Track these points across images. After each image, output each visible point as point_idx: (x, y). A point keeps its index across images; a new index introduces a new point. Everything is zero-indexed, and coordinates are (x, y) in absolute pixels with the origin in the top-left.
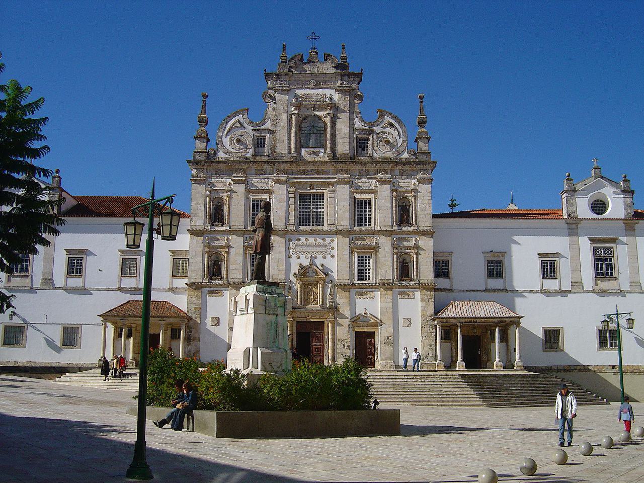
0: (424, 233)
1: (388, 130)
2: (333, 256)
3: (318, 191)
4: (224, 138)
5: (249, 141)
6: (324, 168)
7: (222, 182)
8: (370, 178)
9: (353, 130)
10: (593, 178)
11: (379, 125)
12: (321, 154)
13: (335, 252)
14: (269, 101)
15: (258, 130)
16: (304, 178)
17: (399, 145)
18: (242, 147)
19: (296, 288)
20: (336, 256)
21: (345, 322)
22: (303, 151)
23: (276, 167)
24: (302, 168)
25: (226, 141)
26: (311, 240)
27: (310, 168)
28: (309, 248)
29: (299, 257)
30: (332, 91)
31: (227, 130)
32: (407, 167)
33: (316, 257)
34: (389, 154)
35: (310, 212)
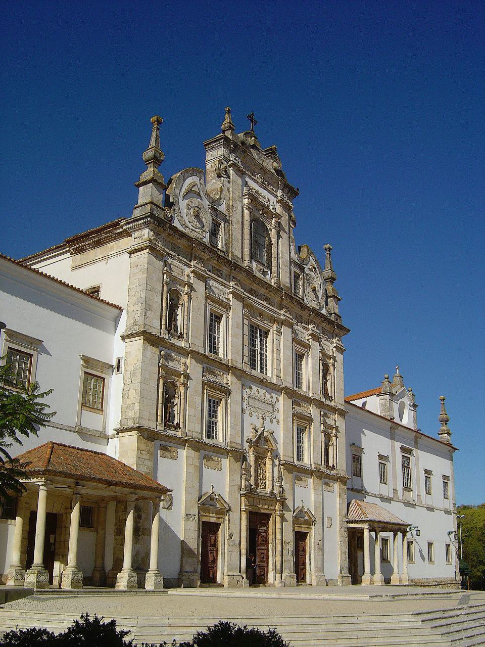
0: (342, 413)
1: (312, 273)
4: (181, 199)
5: (206, 218)
6: (271, 296)
8: (304, 328)
9: (291, 261)
10: (399, 386)
11: (306, 265)
12: (268, 277)
13: (281, 416)
14: (224, 176)
15: (216, 210)
17: (320, 297)
18: (198, 225)
19: (248, 459)
21: (289, 516)
23: (234, 273)
24: (255, 287)
25: (183, 204)
26: (262, 391)
27: (262, 290)
30: (275, 200)
31: (184, 190)
32: (328, 327)
34: (314, 305)
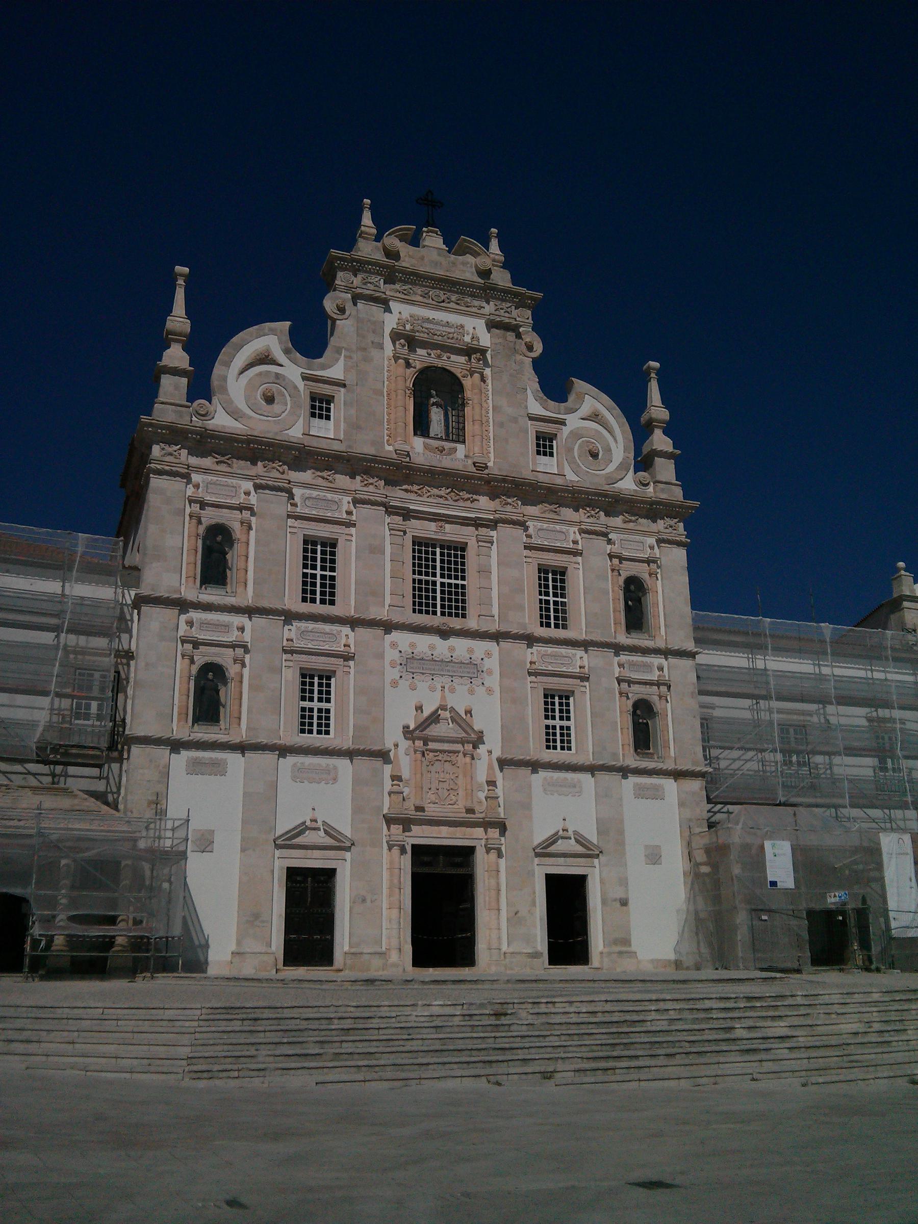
2: (490, 691)
3: (451, 533)
7: (227, 486)
13: (493, 681)
16: (423, 503)
20: (497, 689)
22: (418, 443)
28: (437, 667)
29: (413, 688)
33: (452, 690)
35: (434, 583)
